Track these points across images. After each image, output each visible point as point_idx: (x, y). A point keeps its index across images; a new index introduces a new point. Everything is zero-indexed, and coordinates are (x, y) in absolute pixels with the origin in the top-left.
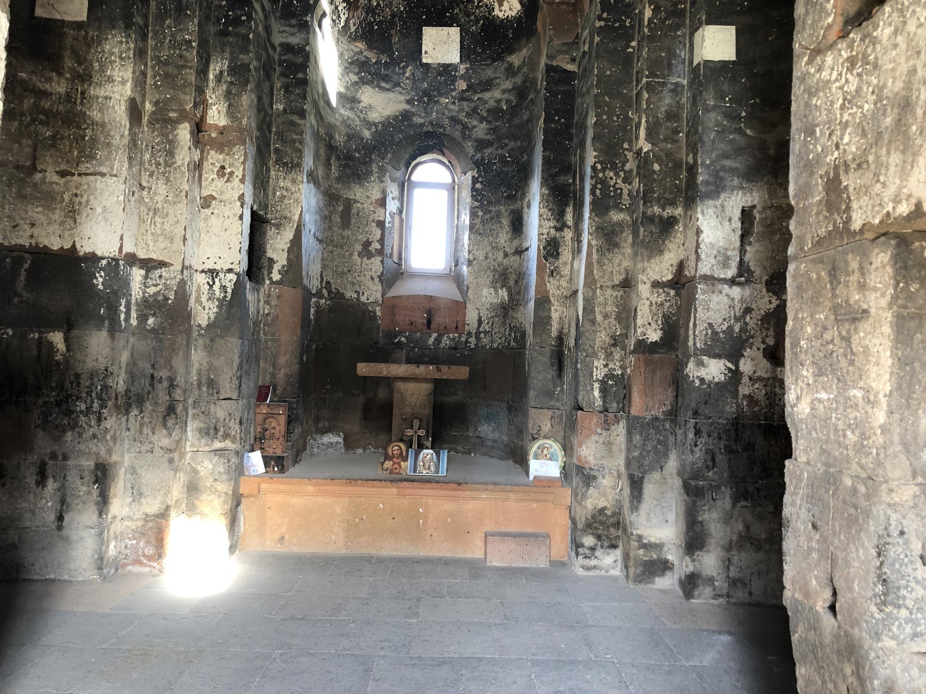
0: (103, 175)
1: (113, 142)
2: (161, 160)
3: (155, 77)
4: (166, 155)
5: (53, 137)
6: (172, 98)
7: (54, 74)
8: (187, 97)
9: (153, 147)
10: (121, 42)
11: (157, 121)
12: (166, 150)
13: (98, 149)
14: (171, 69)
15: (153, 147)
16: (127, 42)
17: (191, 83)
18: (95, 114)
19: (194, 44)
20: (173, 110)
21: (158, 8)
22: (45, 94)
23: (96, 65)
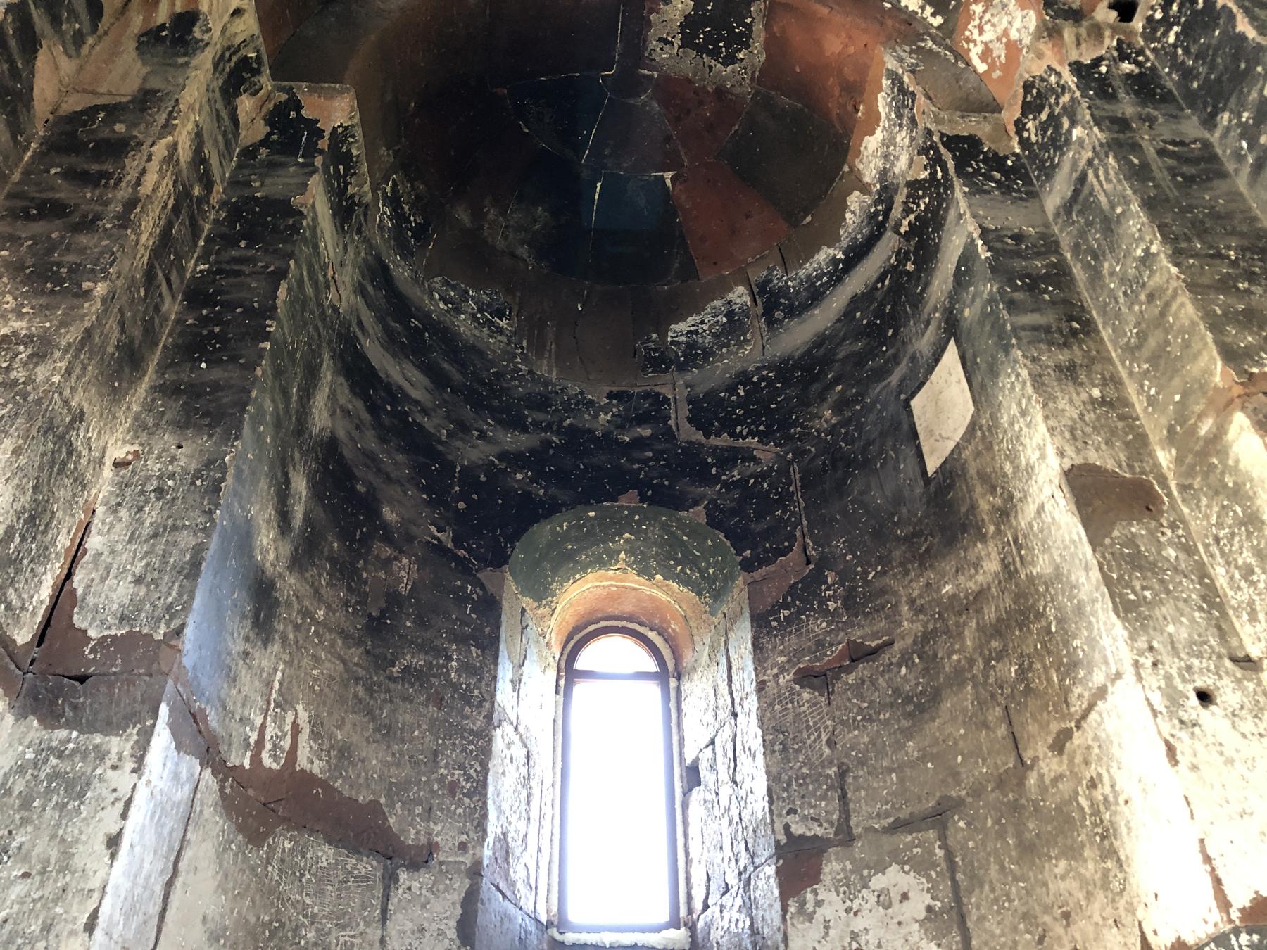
0: (1101, 693)
1: (1083, 596)
2: (1247, 557)
3: (1142, 386)
4: (1249, 534)
5: (1022, 672)
6: (1185, 395)
7: (979, 545)
8: (1203, 362)
9: (1217, 540)
10: (1013, 387)
11: (1191, 472)
12: (1242, 523)
13: (1075, 637)
14: (1152, 342)
15: (1217, 540)
16: (1018, 375)
17: (1193, 324)
18: (1042, 566)
19: (1154, 249)
20: (1200, 417)
21: (1086, 267)
22: (981, 595)
23: (1008, 468)
